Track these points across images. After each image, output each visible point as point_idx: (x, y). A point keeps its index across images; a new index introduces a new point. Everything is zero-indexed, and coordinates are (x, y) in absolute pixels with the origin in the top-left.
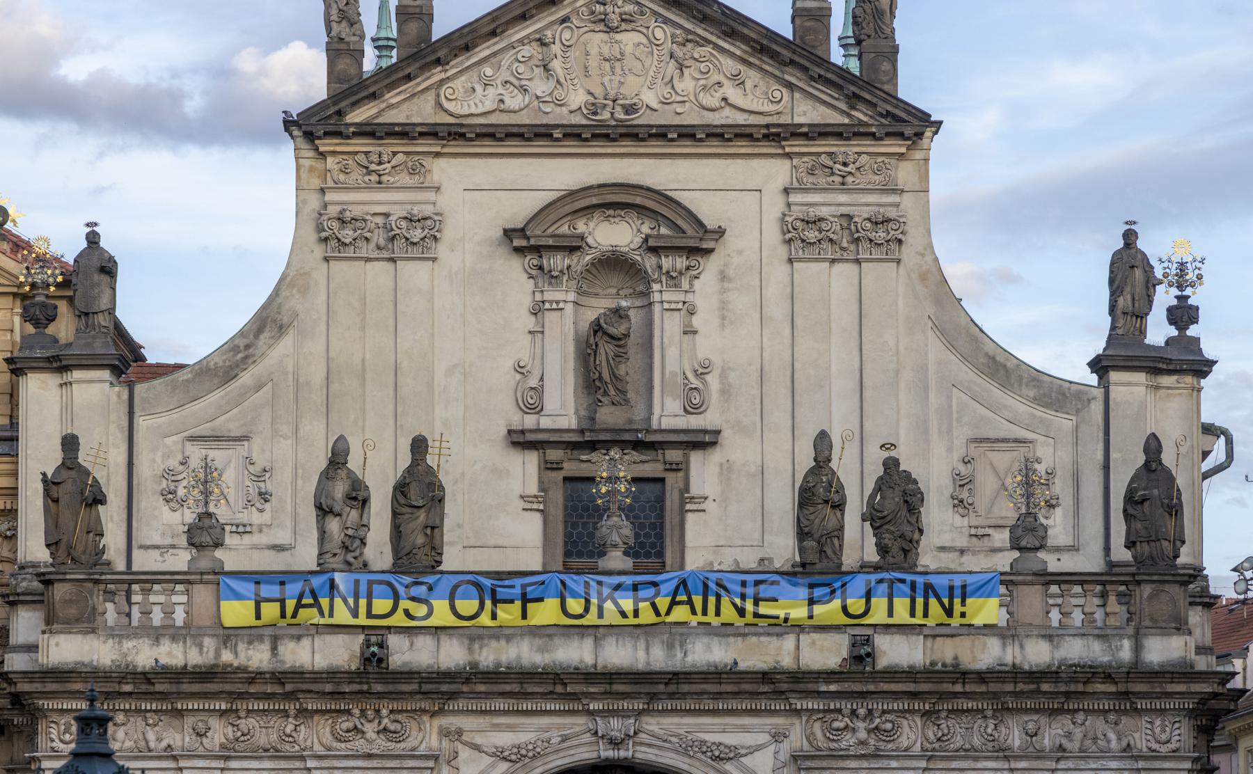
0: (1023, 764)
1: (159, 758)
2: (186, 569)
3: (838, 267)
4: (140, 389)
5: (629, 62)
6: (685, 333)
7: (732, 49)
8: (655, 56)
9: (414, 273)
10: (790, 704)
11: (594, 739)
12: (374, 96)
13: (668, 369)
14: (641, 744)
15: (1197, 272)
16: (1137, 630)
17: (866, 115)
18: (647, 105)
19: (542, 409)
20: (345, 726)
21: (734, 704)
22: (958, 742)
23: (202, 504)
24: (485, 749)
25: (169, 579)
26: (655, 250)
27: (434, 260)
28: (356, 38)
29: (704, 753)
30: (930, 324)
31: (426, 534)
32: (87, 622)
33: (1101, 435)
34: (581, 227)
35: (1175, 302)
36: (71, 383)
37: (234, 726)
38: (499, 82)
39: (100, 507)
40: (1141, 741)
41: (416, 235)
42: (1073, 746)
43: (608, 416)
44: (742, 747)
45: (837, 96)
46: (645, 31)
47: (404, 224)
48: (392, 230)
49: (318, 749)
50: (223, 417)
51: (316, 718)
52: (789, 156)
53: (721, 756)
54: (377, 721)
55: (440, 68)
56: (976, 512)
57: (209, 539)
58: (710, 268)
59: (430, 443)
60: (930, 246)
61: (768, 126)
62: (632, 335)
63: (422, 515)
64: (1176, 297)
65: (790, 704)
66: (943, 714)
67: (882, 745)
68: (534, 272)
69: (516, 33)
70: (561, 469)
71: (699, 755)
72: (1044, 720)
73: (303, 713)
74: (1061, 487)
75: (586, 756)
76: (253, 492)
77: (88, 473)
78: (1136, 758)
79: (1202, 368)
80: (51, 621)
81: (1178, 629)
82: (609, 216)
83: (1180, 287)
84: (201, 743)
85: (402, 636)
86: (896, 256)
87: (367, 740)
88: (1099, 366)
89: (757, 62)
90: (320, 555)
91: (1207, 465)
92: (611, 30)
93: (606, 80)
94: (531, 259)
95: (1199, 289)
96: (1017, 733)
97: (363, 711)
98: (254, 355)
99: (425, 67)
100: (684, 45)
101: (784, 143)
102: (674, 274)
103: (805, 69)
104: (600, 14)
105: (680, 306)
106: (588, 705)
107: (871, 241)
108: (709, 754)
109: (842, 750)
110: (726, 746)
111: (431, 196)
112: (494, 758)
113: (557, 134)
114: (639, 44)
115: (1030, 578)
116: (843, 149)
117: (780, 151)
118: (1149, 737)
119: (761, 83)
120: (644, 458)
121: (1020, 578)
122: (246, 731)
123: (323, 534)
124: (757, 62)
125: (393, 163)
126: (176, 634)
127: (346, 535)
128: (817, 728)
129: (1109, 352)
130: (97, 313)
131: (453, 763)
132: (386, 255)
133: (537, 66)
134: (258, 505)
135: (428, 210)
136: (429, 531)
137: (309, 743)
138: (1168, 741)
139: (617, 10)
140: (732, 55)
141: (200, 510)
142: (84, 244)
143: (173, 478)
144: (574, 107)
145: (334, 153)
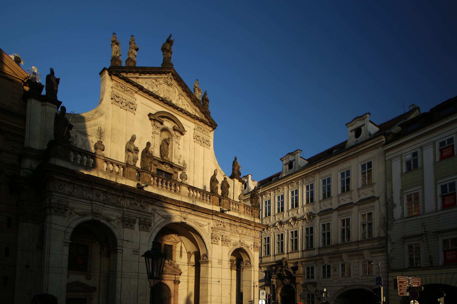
10: (213, 218)
20: (133, 202)
49: (126, 206)
65: (213, 218)
73: (124, 197)
75: (178, 220)
89: (191, 104)
94: (153, 122)
97: (137, 200)
112: (161, 217)
124: (191, 104)
128: (215, 223)
131: (154, 216)
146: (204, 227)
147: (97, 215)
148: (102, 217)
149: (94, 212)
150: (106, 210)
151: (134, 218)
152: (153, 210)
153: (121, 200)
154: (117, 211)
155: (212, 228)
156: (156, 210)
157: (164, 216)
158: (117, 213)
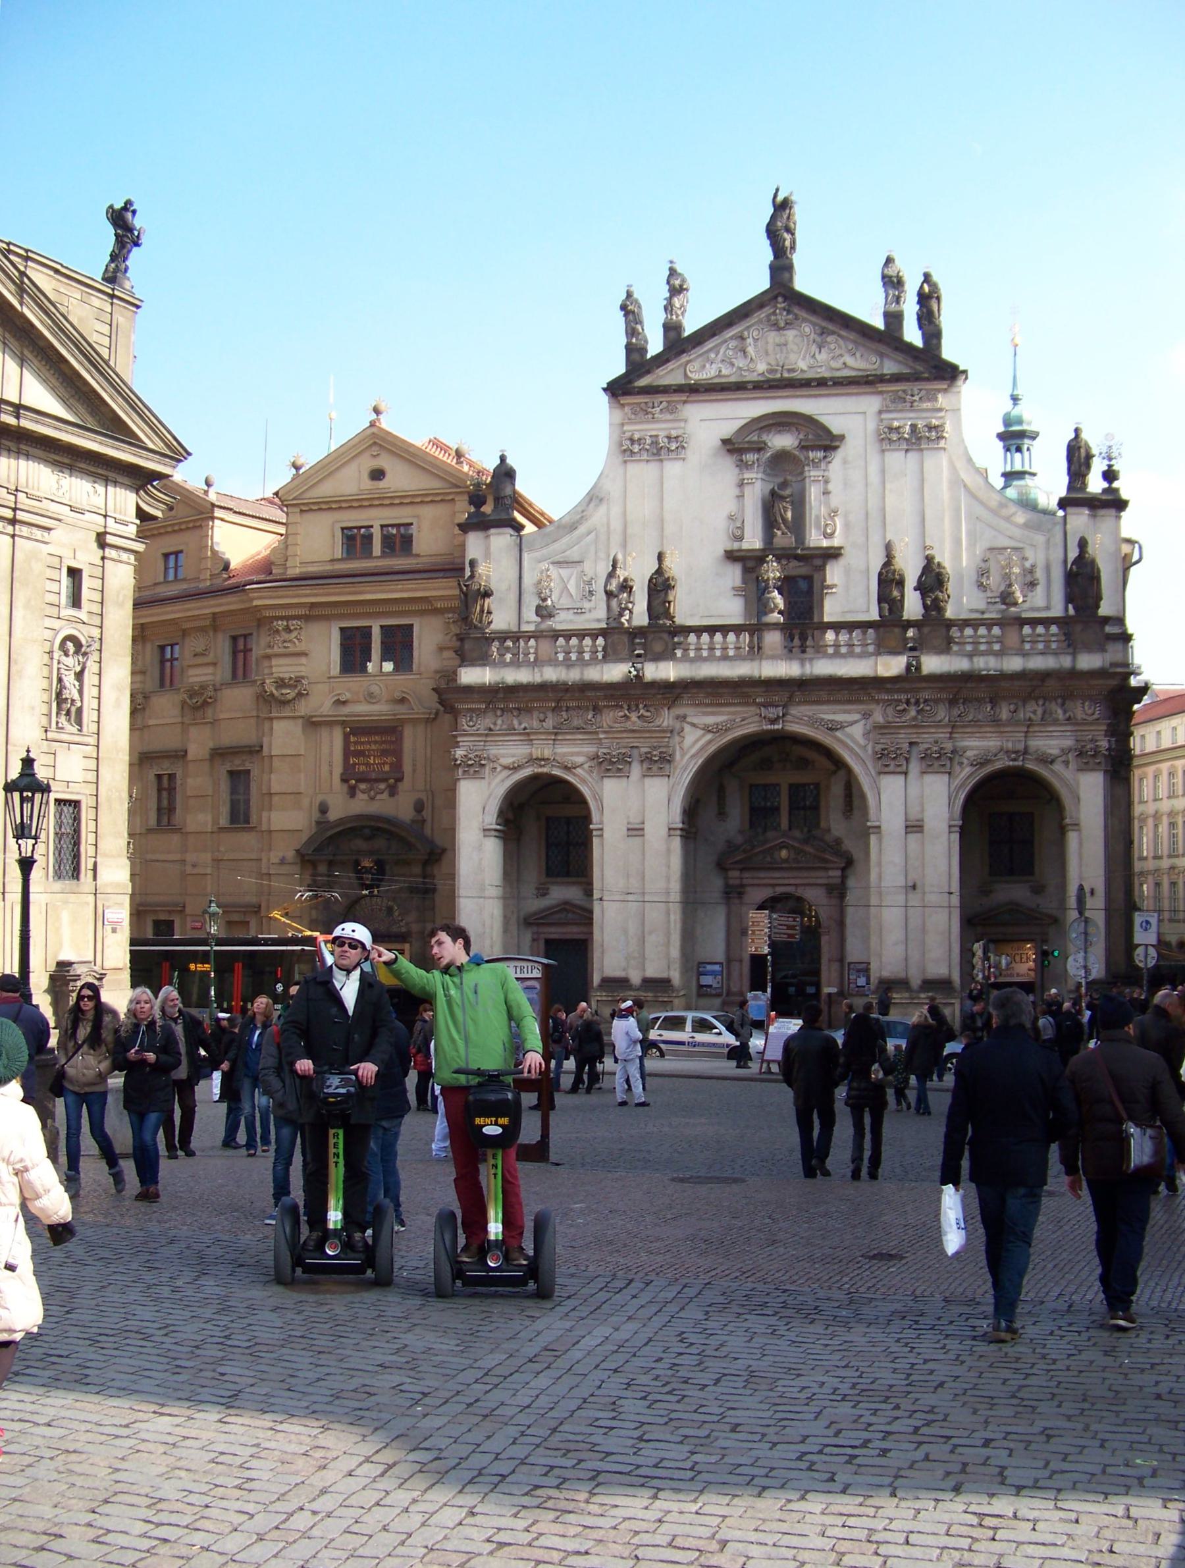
1: (520, 734)
3: (910, 454)
5: (791, 346)
9: (673, 469)
12: (648, 372)
25: (529, 636)
27: (684, 459)
32: (482, 660)
34: (764, 437)
40: (1080, 715)
41: (673, 446)
50: (568, 553)
52: (881, 393)
53: (833, 728)
58: (838, 457)
60: (963, 441)
61: (868, 376)
72: (1020, 704)
74: (1040, 574)
79: (1120, 505)
83: (1110, 459)
88: (1063, 503)
95: (1119, 460)
103: (888, 344)
111: (682, 424)
128: (890, 710)
135: (680, 432)
145: (629, 404)
146: (848, 730)
151: (623, 751)
152: (677, 718)
155: (878, 727)
156: (685, 717)
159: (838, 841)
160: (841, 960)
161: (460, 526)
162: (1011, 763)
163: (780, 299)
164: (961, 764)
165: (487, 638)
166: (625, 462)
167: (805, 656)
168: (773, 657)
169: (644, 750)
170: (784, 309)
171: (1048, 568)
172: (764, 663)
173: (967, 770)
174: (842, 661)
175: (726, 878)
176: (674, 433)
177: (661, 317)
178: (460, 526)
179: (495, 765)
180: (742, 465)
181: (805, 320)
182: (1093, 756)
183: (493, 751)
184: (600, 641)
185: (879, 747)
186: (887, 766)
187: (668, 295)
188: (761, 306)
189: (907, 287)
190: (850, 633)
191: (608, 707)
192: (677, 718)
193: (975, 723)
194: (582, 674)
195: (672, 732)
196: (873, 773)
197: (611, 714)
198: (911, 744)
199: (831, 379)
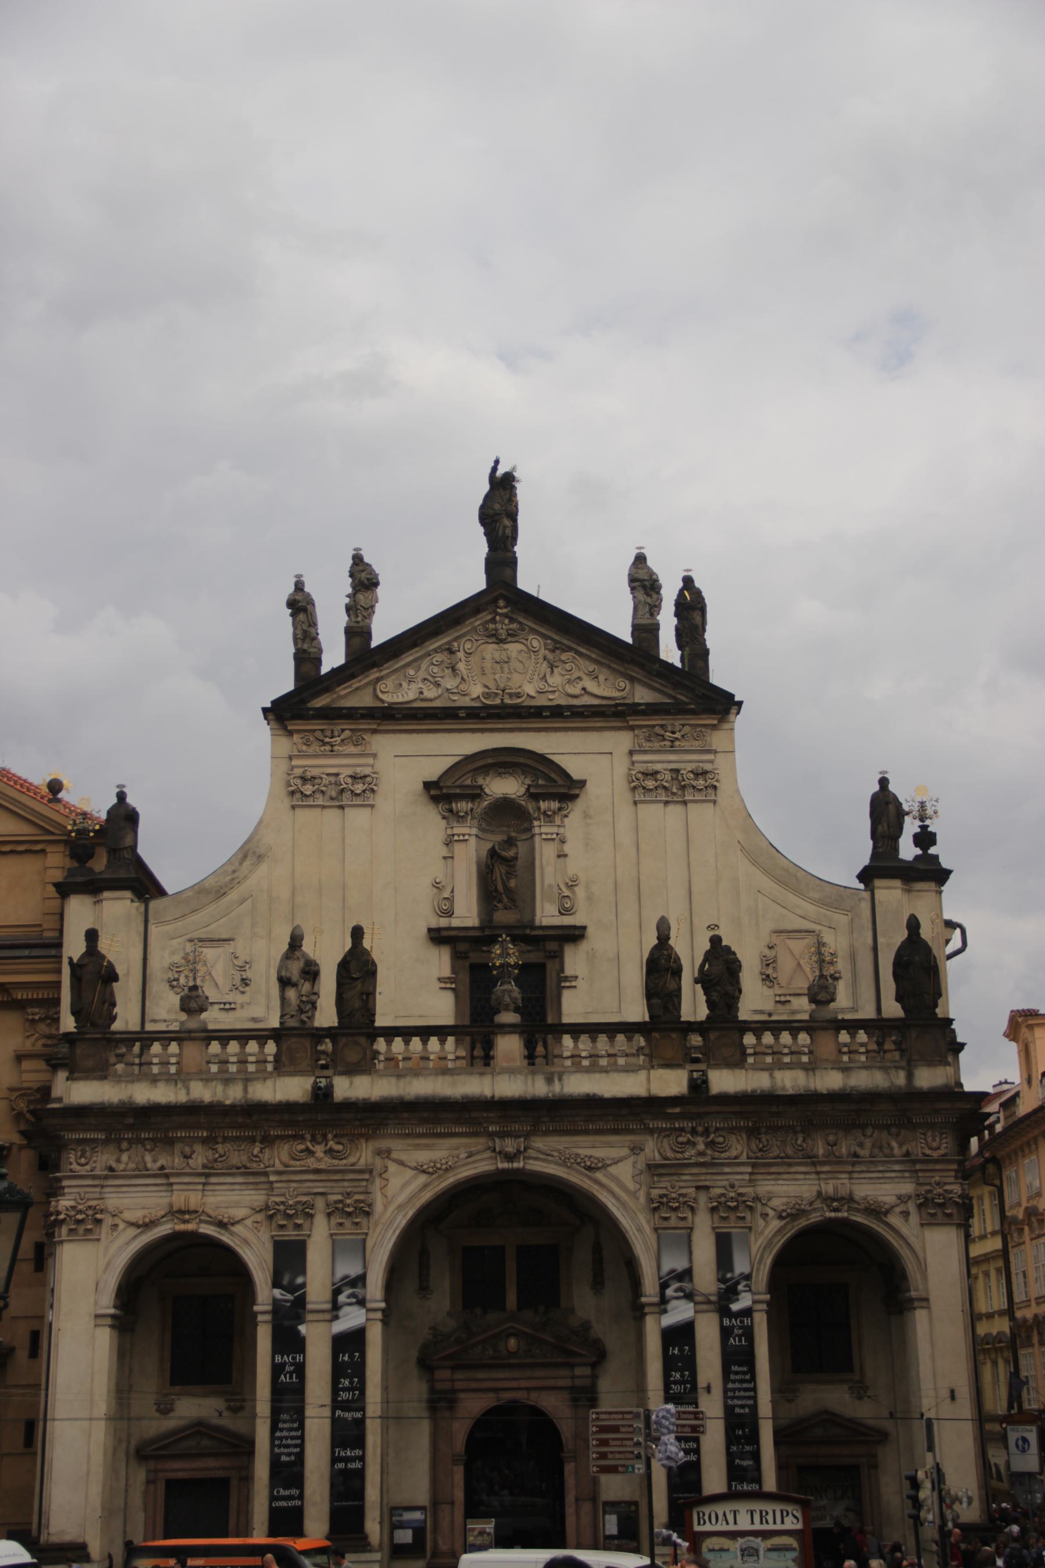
0: (826, 1168)
1: (155, 1176)
2: (177, 1029)
3: (671, 808)
4: (154, 904)
5: (515, 664)
6: (559, 856)
7: (588, 653)
8: (533, 660)
9: (357, 817)
10: (645, 1124)
11: (493, 1154)
12: (327, 690)
13: (547, 882)
14: (530, 1158)
15: (933, 808)
16: (909, 1062)
17: (686, 697)
18: (528, 695)
19: (453, 914)
21: (601, 1125)
22: (776, 1152)
23: (191, 979)
24: (409, 1164)
25: (165, 1038)
26: (535, 797)
27: (372, 806)
28: (315, 650)
29: (579, 1164)
30: (739, 847)
31: (362, 999)
32: (101, 1072)
33: (870, 926)
34: (480, 781)
35: (919, 830)
36: (102, 901)
37: (213, 1149)
38: (419, 679)
39: (114, 984)
41: (359, 788)
42: (864, 1153)
43: (503, 917)
44: (608, 1159)
45: (665, 684)
46: (524, 641)
47: (349, 780)
48: (341, 785)
49: (279, 1166)
50: (213, 926)
51: (277, 1142)
52: (632, 728)
54: (324, 1144)
55: (375, 669)
56: (778, 984)
57: (195, 1005)
58: (576, 811)
59: (365, 931)
60: (738, 791)
61: (617, 705)
62: (519, 860)
63: (359, 984)
64: (920, 827)
65: (645, 1124)
66: (763, 1130)
67: (716, 1154)
68: (446, 814)
69: (431, 644)
70: (467, 958)
71: (575, 1165)
76: (238, 981)
77: (103, 957)
78: (914, 1162)
79: (941, 876)
80: (76, 1072)
81: (940, 1061)
82: (500, 773)
83: (922, 819)
84: (188, 1164)
85: (344, 1077)
86: (713, 798)
87: (316, 1158)
88: (866, 876)
90: (282, 1016)
91: (950, 949)
92: (500, 641)
93: (497, 677)
95: (935, 820)
96: (820, 1144)
98: (238, 878)
99: (366, 669)
100: (553, 651)
101: (628, 718)
102: (550, 813)
103: (642, 666)
104: (493, 630)
105: (554, 836)
106: (488, 1127)
107: (694, 787)
108: (583, 1164)
109: (686, 1159)
110: (595, 1158)
111: (370, 761)
113: (462, 714)
114: (521, 651)
115: (824, 1024)
116: (672, 722)
117: (625, 724)
118: (923, 1145)
119: (611, 677)
120: (529, 948)
121: (818, 1024)
122: (223, 1153)
123: (283, 999)
125: (342, 737)
126: (173, 1080)
127: (301, 1001)
129: (873, 864)
130: (122, 849)
131: (383, 1176)
132: (337, 804)
133: (447, 668)
134: (242, 990)
135: (367, 771)
136: (364, 997)
137: (271, 1162)
138: (938, 1148)
139: (504, 627)
140: (589, 658)
141: (191, 984)
142: (115, 800)
143: (178, 970)
144: (474, 696)
146: (612, 1170)
147: (187, 1217)
148: (203, 1218)
149: (175, 1209)
150: (217, 1193)
151: (304, 1199)
153: (262, 1149)
154: (250, 1187)
155: (649, 1167)
156: (389, 1152)
157: (422, 1166)
158: (252, 1192)
159: (586, 1326)
160: (594, 1499)
161: (57, 885)
162: (833, 1215)
163: (501, 603)
164: (765, 1216)
165: (109, 1041)
166: (293, 807)
167: (553, 1069)
168: (512, 1071)
169: (333, 1198)
170: (506, 616)
171: (853, 957)
172: (498, 1078)
173: (775, 1224)
174: (604, 1075)
175: (432, 1381)
176: (360, 771)
177: (342, 619)
178: (57, 885)
179: (117, 1221)
180: (452, 816)
181: (533, 631)
182: (942, 1206)
183: (113, 1200)
184: (271, 1047)
185: (655, 1192)
186: (666, 1219)
187: (350, 590)
188: (477, 611)
189: (662, 592)
190: (612, 1038)
191: (282, 1138)
192: (379, 1153)
193: (785, 1161)
194: (245, 1090)
195: (371, 1172)
196: (647, 1229)
197: (286, 1147)
198: (698, 1188)
199: (569, 707)
